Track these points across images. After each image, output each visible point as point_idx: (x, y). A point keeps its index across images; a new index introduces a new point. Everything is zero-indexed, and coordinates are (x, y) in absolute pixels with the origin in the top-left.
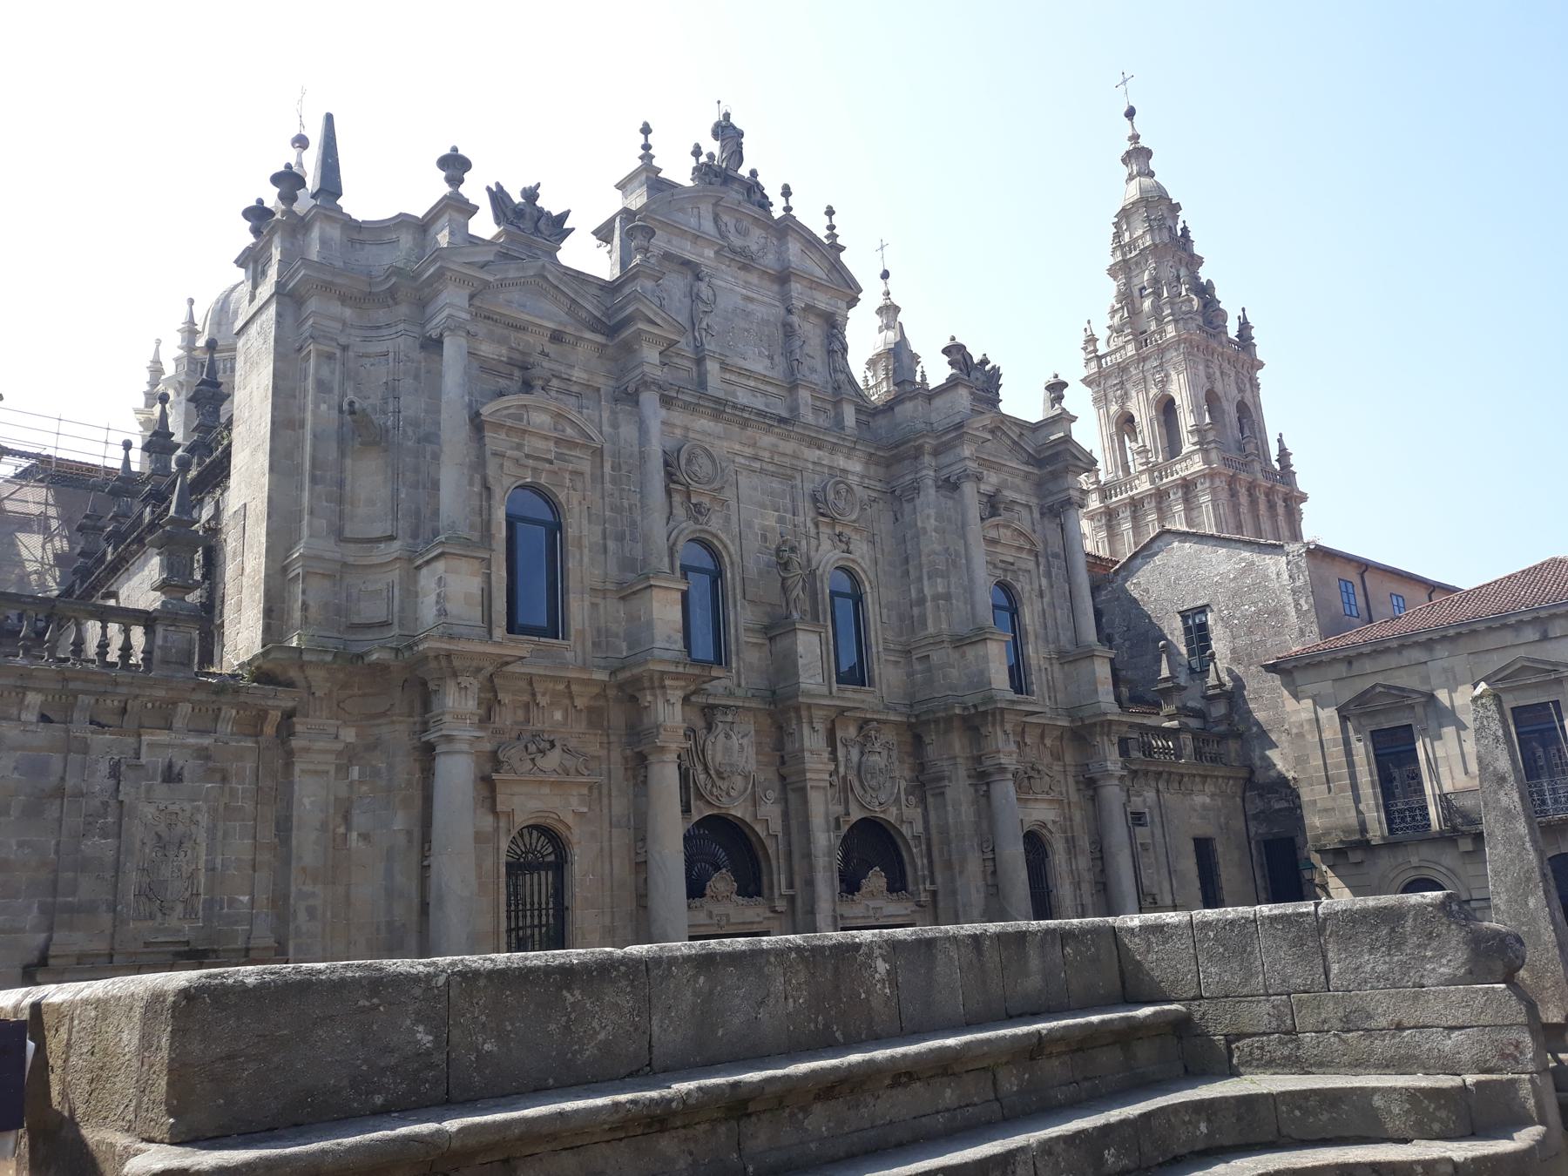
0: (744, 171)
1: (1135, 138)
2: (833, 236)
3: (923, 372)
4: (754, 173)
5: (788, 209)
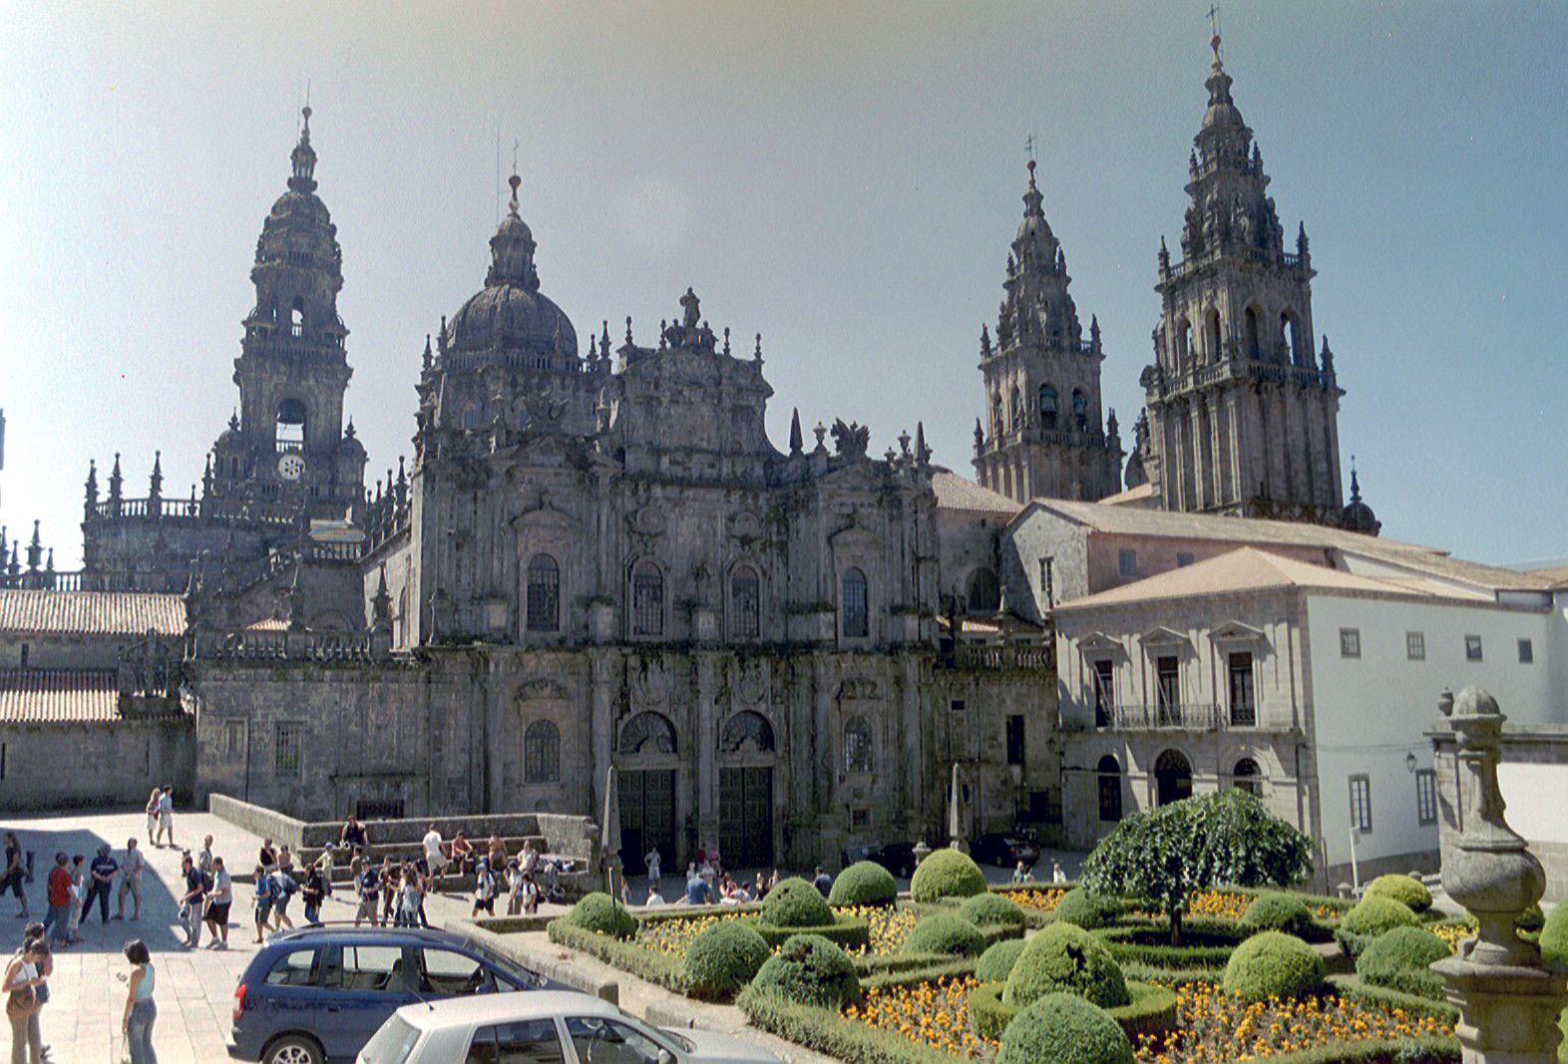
0: (700, 325)
1: (1218, 66)
2: (758, 355)
3: (1061, 252)
4: (706, 324)
5: (727, 344)
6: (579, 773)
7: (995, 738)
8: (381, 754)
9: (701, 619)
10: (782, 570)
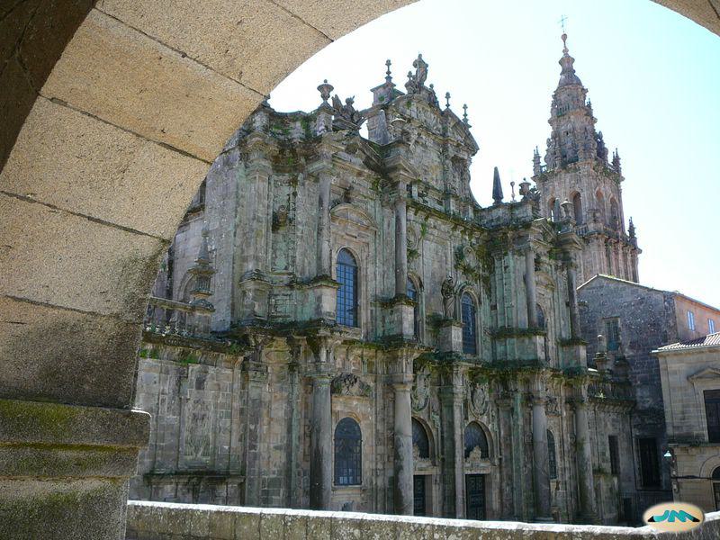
1: (565, 51)
2: (466, 120)
4: (432, 86)
5: (448, 105)
6: (377, 476)
7: (604, 454)
8: (197, 450)
9: (453, 332)
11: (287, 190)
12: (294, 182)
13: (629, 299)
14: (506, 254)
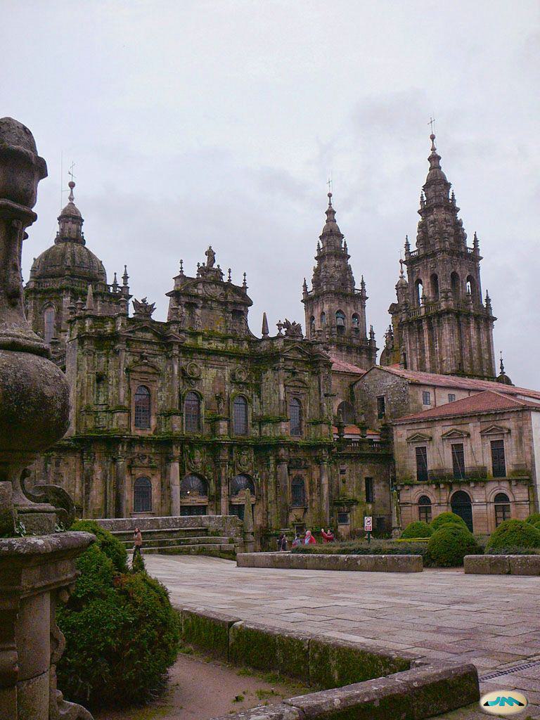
0: (215, 266)
2: (245, 284)
4: (218, 266)
5: (230, 277)
10: (258, 400)
11: (104, 359)
12: (107, 355)
13: (391, 383)
14: (267, 370)
